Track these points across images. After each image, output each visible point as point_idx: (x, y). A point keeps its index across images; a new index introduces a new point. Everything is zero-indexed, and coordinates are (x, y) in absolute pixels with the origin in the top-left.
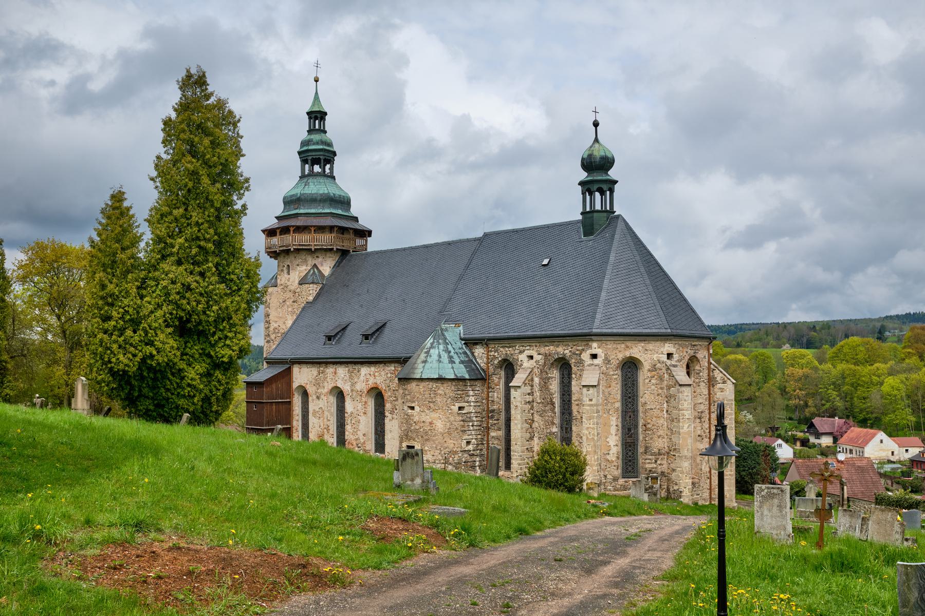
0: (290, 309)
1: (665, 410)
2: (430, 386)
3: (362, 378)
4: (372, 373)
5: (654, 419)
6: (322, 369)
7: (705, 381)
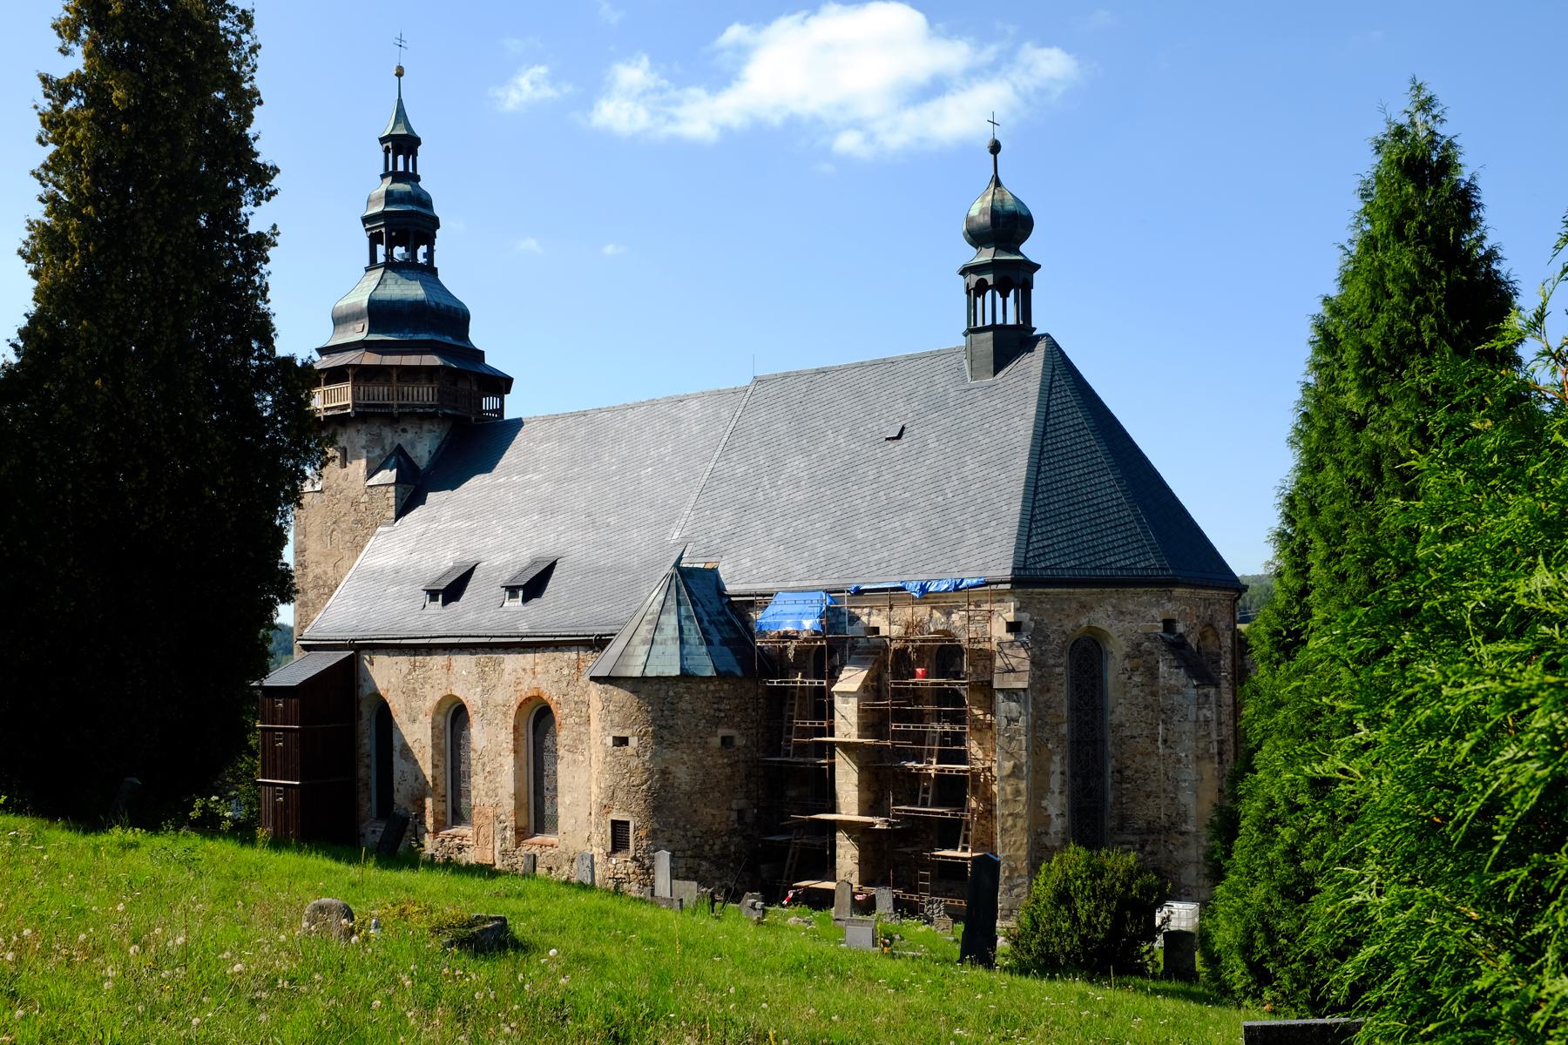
0: (347, 538)
1: (1160, 739)
2: (662, 694)
3: (506, 677)
4: (528, 667)
5: (1139, 758)
7: (1229, 677)
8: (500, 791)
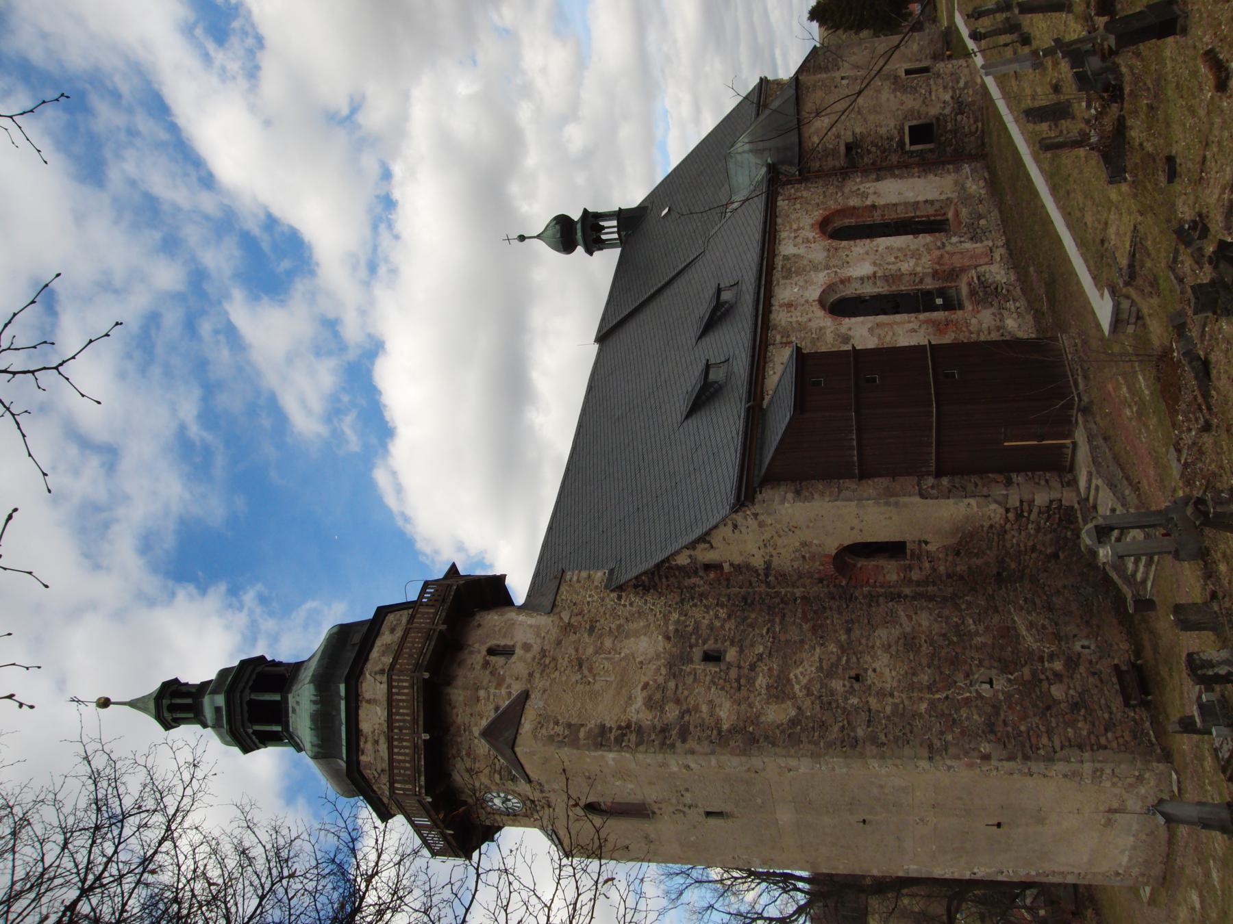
0: (608, 643)
3: (801, 251)
4: (793, 235)
6: (778, 338)
8: (912, 247)
